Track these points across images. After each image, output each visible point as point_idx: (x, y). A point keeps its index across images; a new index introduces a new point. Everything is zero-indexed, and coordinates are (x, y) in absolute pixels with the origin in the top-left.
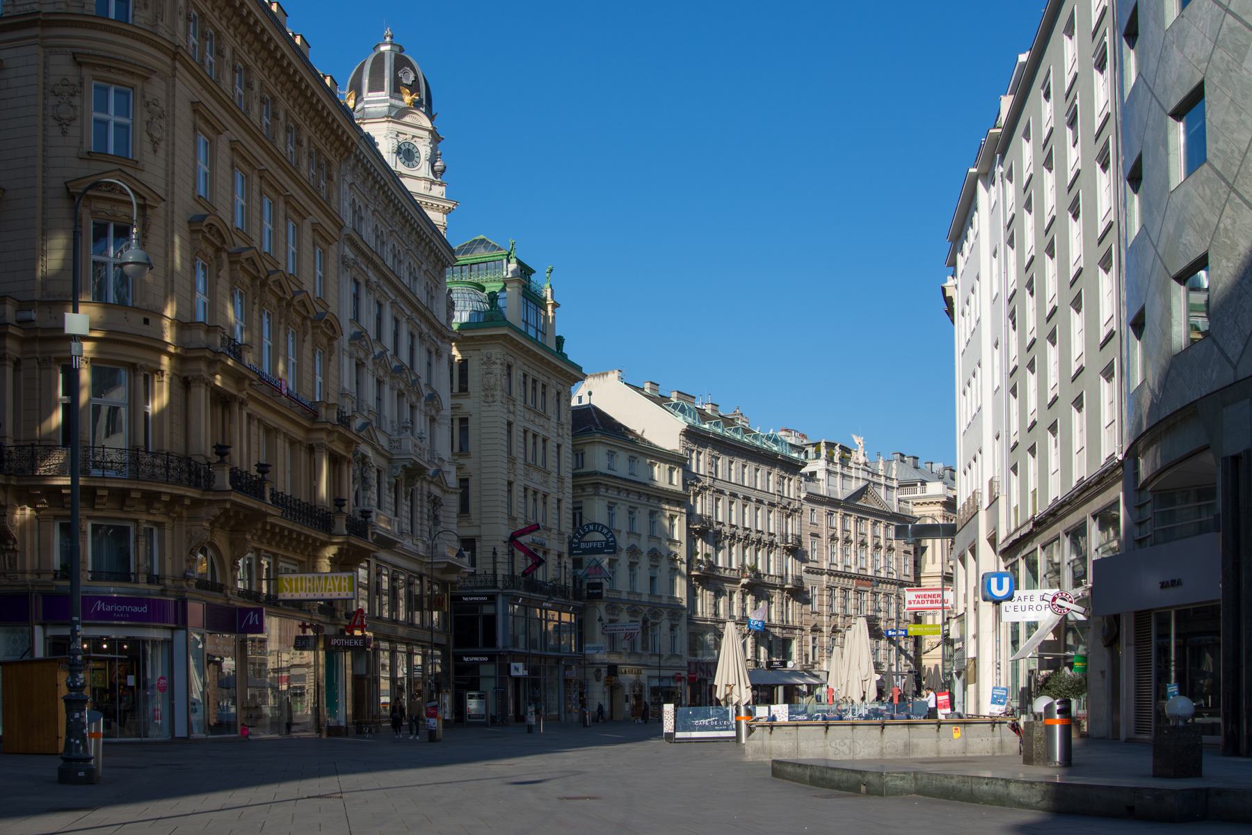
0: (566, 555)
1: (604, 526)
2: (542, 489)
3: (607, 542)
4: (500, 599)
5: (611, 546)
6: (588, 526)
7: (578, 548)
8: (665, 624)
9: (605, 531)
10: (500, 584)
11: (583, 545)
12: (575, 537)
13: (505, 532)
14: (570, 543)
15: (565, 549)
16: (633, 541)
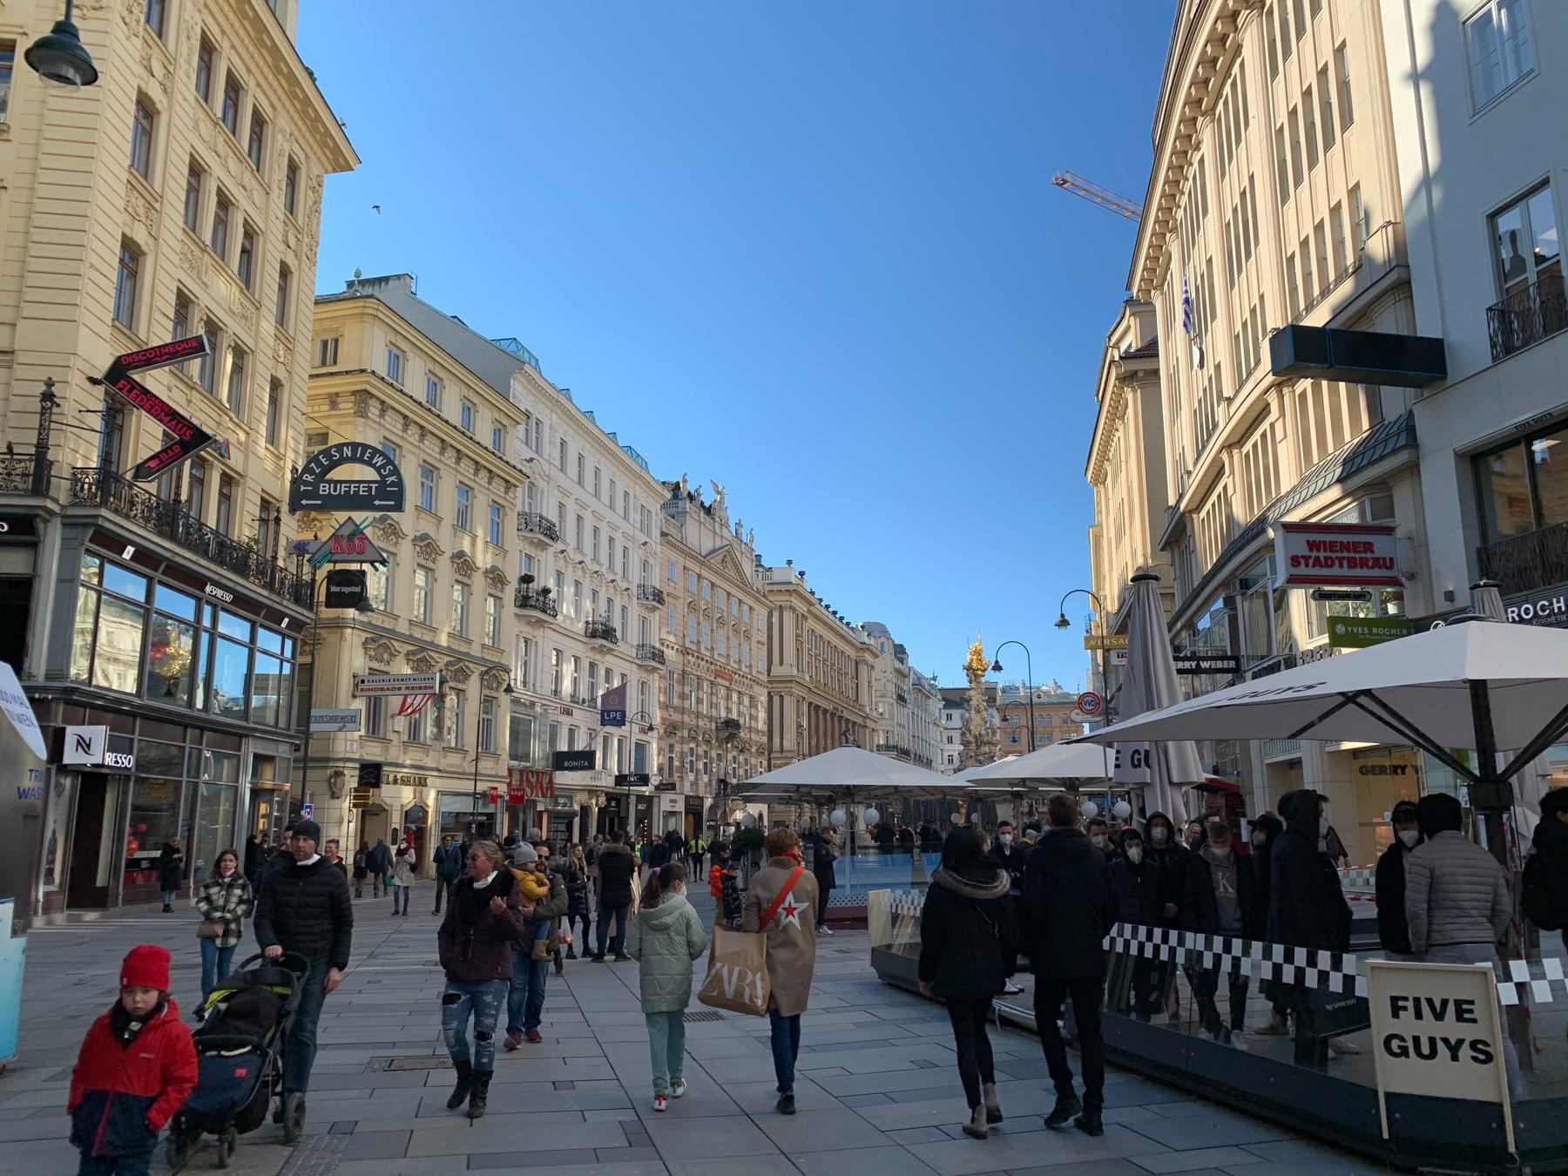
0: (285, 508)
1: (375, 451)
2: (233, 328)
3: (382, 483)
4: (53, 538)
5: (389, 494)
6: (339, 447)
7: (313, 494)
8: (473, 686)
9: (379, 461)
10: (61, 490)
11: (324, 489)
12: (306, 469)
13: (101, 354)
14: (295, 482)
15: (281, 489)
16: (426, 526)
